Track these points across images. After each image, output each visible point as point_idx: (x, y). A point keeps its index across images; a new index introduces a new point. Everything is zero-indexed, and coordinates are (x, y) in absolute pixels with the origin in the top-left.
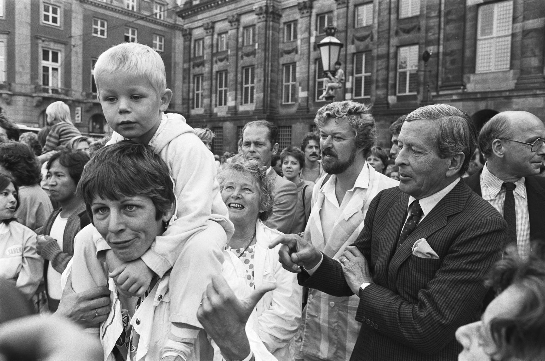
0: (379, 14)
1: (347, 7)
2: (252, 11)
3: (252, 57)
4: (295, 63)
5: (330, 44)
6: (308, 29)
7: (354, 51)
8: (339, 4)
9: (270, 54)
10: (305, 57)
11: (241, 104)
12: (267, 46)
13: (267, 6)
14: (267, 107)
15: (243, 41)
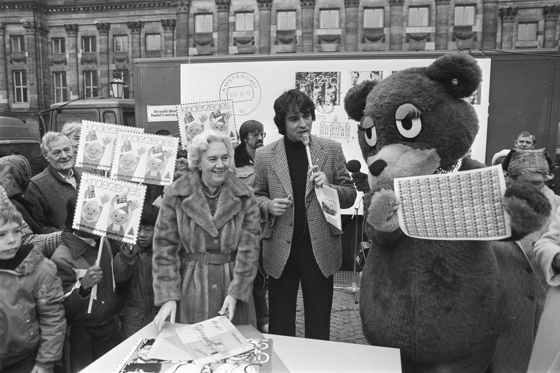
0: (132, 45)
1: (108, 36)
2: (19, 23)
3: (22, 63)
4: (65, 72)
5: (118, 83)
6: (75, 47)
7: (115, 69)
8: (101, 32)
9: (41, 63)
10: (74, 69)
11: (14, 102)
12: (38, 57)
13: (34, 22)
14: (42, 106)
15: (11, 48)
